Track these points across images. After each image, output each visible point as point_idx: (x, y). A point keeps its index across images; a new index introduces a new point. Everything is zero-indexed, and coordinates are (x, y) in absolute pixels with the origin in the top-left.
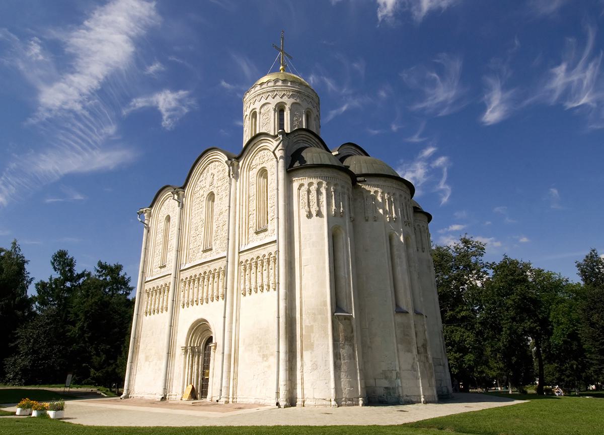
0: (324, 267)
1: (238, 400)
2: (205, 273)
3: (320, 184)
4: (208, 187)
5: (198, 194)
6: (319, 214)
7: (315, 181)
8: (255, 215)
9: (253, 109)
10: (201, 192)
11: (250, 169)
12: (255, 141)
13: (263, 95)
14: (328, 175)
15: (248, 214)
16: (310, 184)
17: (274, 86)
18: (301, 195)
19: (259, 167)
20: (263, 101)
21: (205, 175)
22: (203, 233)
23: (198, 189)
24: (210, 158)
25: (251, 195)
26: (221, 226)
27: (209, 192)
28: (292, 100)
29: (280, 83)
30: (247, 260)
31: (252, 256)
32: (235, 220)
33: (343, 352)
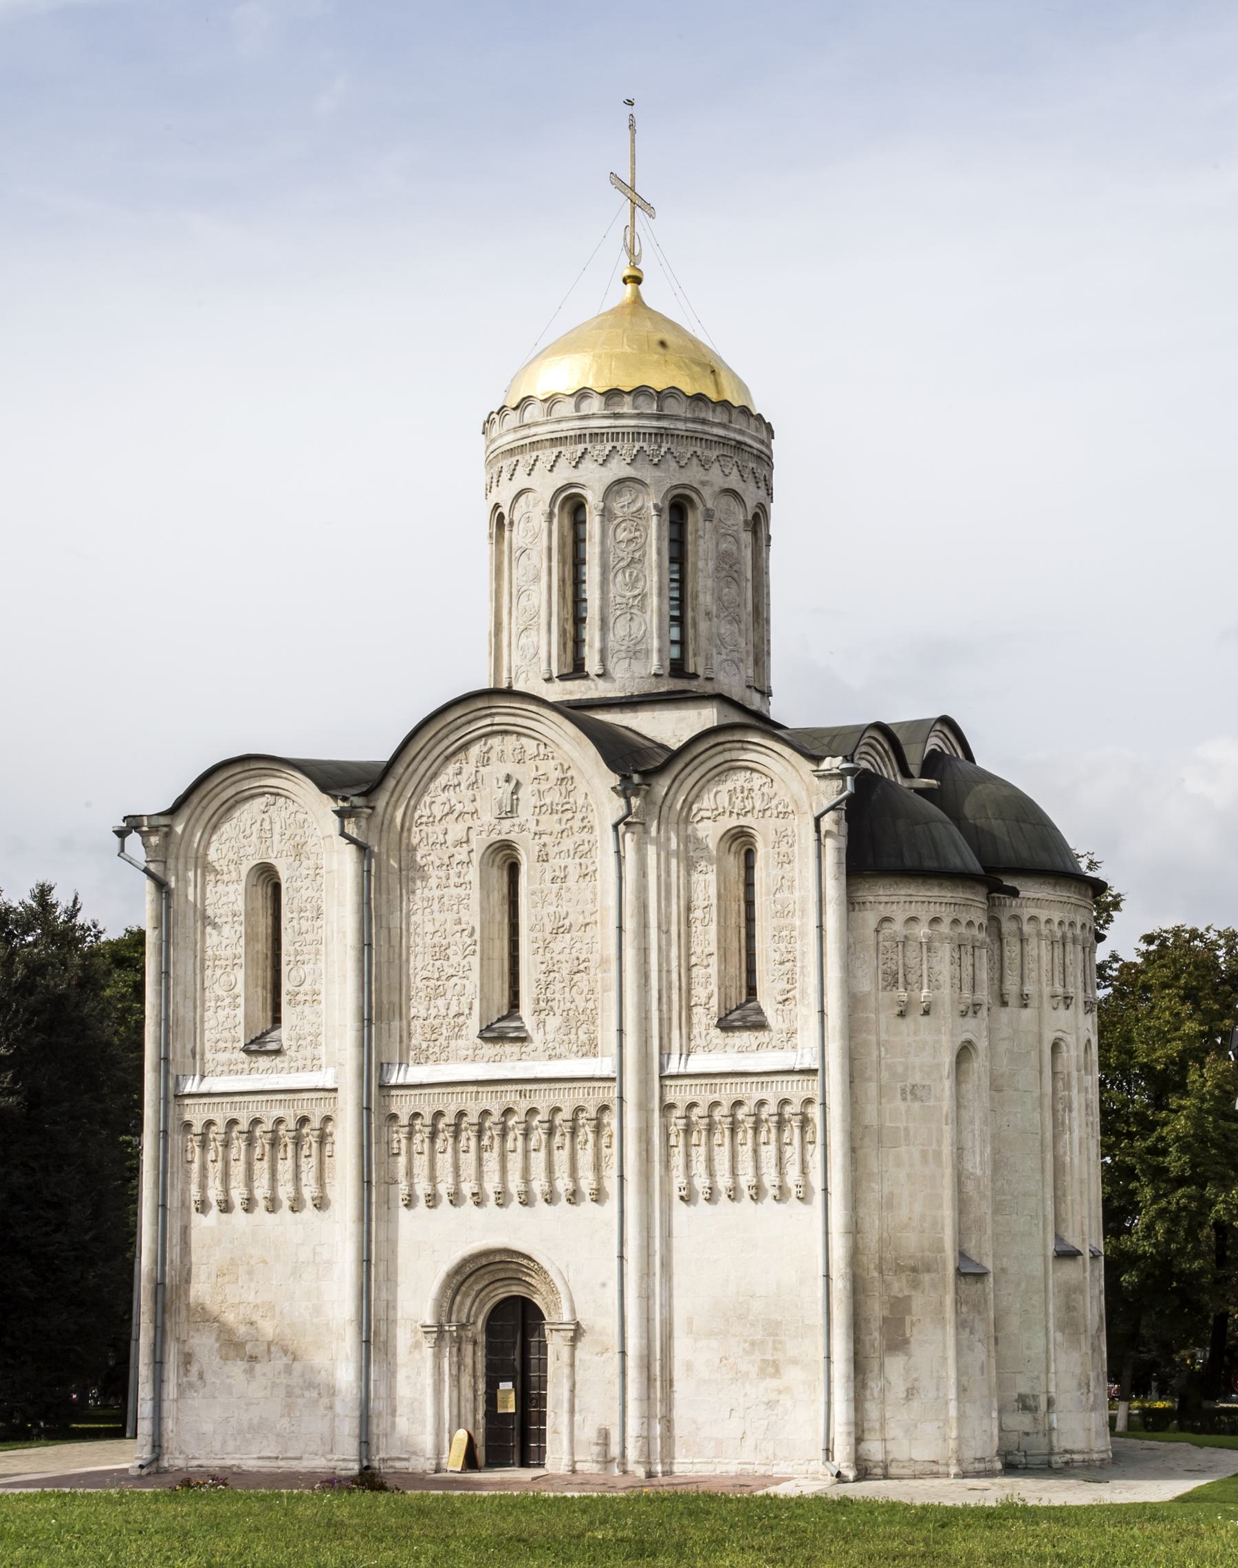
1: (676, 1468)
2: (508, 1112)
4: (488, 817)
5: (439, 828)
7: (925, 914)
8: (713, 970)
9: (571, 485)
12: (721, 739)
13: (618, 445)
15: (688, 961)
17: (659, 417)
18: (881, 948)
19: (734, 822)
21: (469, 769)
22: (475, 976)
23: (438, 811)
24: (497, 719)
25: (699, 901)
26: (565, 972)
27: (495, 837)
30: (692, 1105)
31: (716, 1097)
32: (644, 976)
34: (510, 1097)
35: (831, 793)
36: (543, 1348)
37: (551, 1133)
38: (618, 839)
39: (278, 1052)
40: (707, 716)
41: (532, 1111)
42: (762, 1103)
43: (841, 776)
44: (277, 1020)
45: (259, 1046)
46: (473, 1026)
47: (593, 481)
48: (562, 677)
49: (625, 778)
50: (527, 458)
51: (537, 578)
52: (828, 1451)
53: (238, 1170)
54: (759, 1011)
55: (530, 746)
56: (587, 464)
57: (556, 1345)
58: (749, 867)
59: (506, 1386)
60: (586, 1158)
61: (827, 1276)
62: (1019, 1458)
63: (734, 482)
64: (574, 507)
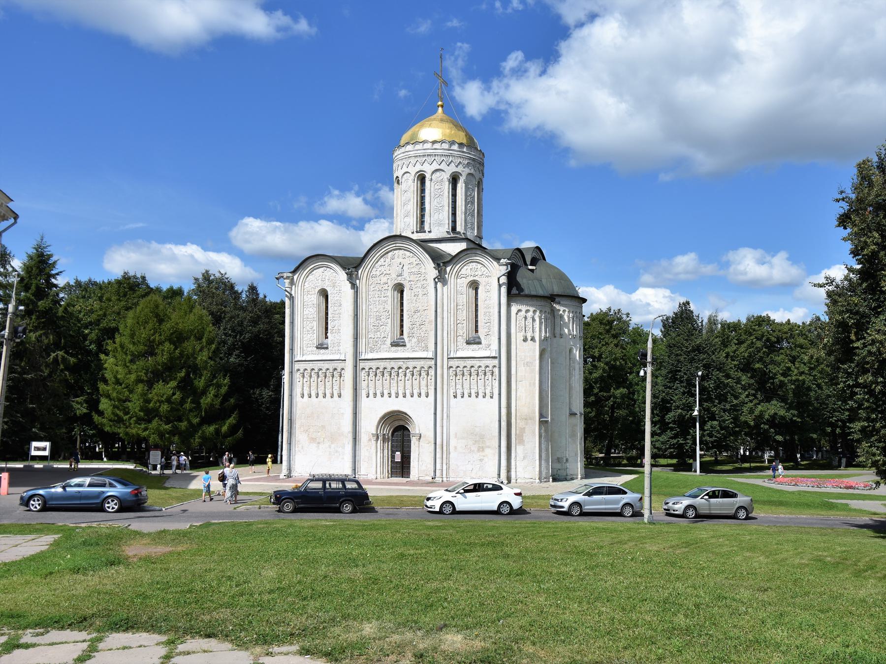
0: (534, 384)
3: (534, 312)
4: (394, 276)
6: (533, 339)
7: (532, 309)
8: (465, 325)
10: (384, 279)
11: (457, 276)
14: (539, 303)
16: (527, 311)
19: (472, 278)
20: (435, 166)
21: (388, 260)
28: (467, 171)
29: (455, 147)
33: (543, 446)
34: (400, 363)
35: (504, 270)
36: (410, 441)
37: (413, 375)
38: (436, 283)
39: (327, 348)
40: (463, 246)
41: (407, 368)
42: (480, 367)
43: (506, 265)
44: (327, 337)
45: (321, 347)
46: (389, 342)
47: (428, 169)
48: (417, 232)
49: (438, 265)
50: (406, 162)
51: (409, 200)
52: (499, 475)
53: (314, 385)
54: (479, 338)
55: (408, 254)
56: (426, 164)
57: (414, 440)
58: (476, 294)
59: (398, 453)
60: (423, 383)
61: (500, 421)
62: (557, 476)
63: (472, 171)
64: (422, 179)
